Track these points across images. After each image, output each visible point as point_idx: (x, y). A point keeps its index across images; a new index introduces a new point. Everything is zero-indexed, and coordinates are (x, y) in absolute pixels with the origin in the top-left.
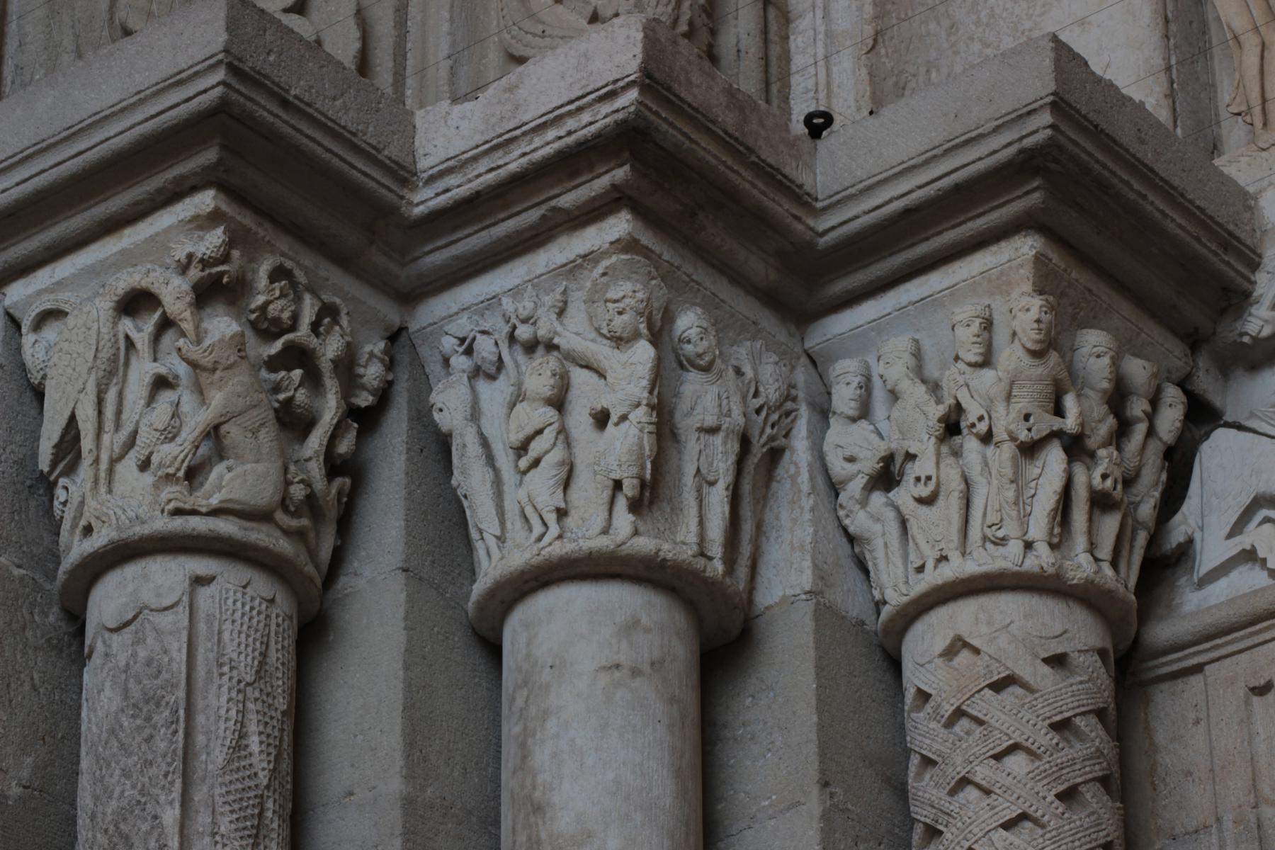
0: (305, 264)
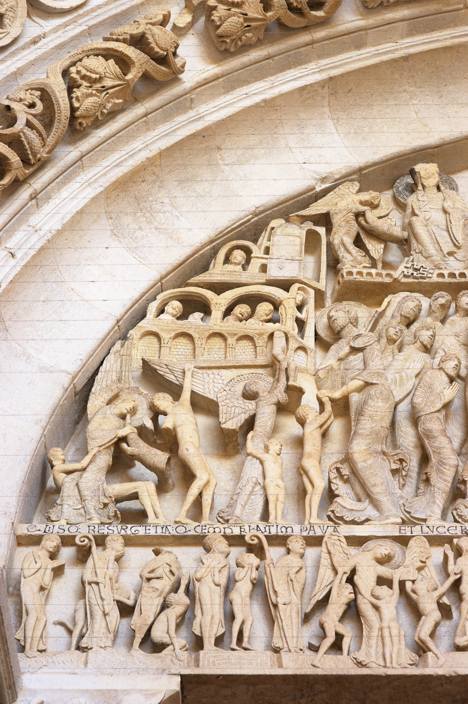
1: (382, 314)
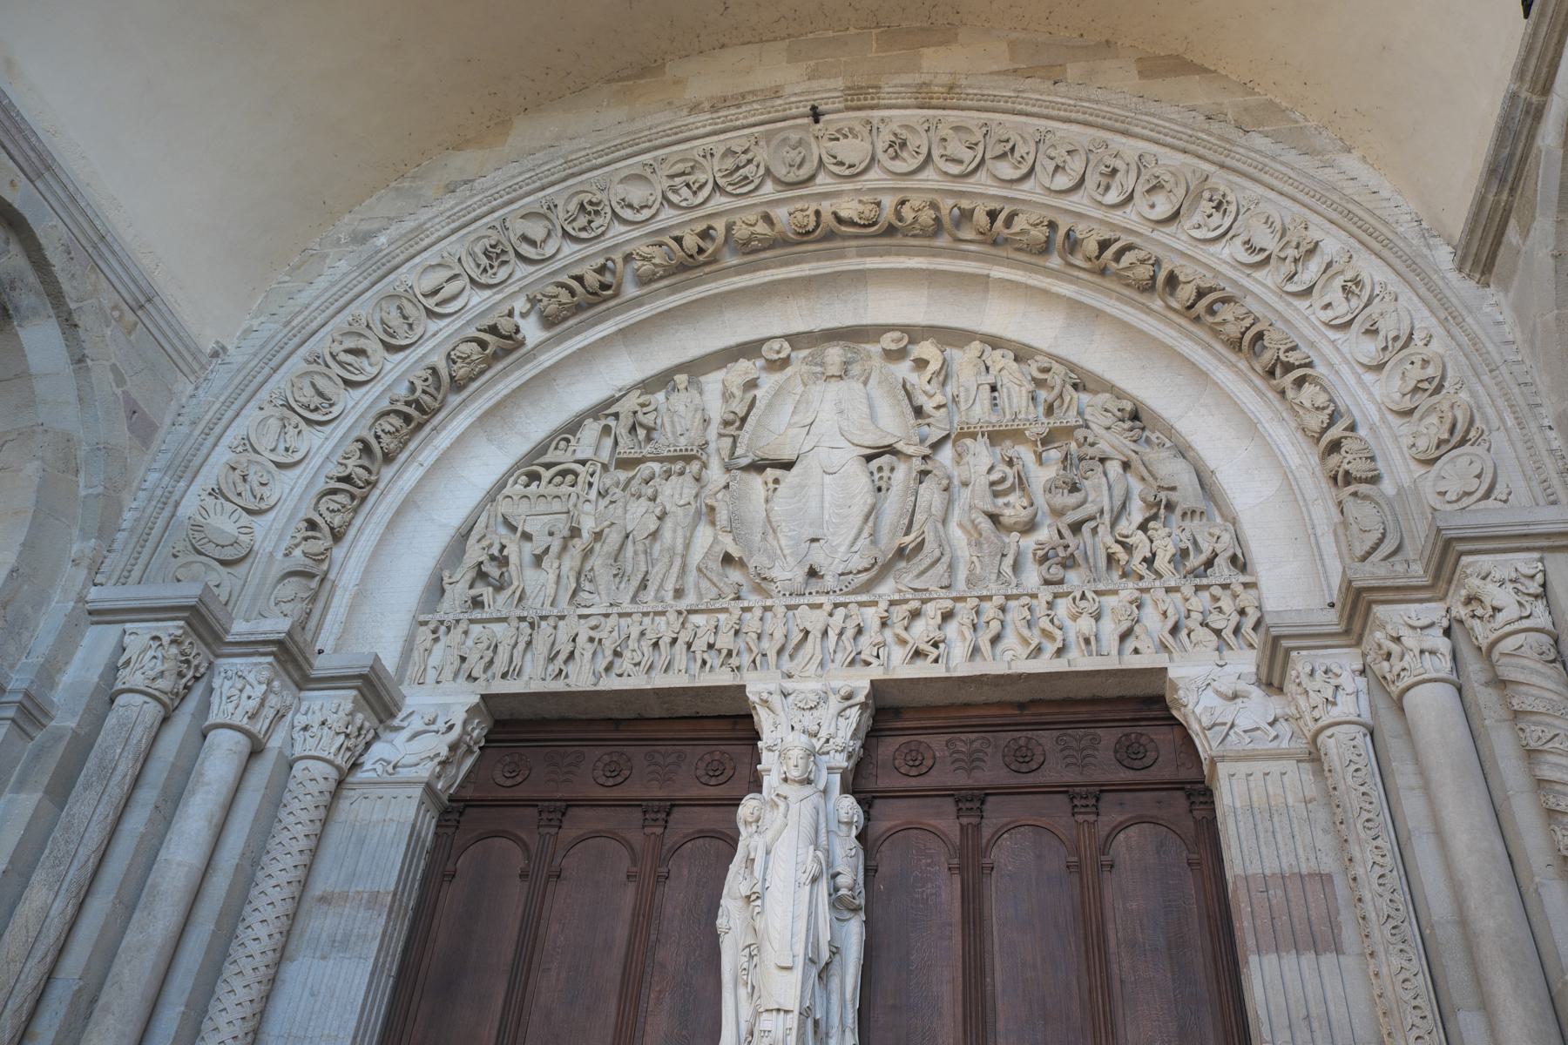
1: (633, 478)
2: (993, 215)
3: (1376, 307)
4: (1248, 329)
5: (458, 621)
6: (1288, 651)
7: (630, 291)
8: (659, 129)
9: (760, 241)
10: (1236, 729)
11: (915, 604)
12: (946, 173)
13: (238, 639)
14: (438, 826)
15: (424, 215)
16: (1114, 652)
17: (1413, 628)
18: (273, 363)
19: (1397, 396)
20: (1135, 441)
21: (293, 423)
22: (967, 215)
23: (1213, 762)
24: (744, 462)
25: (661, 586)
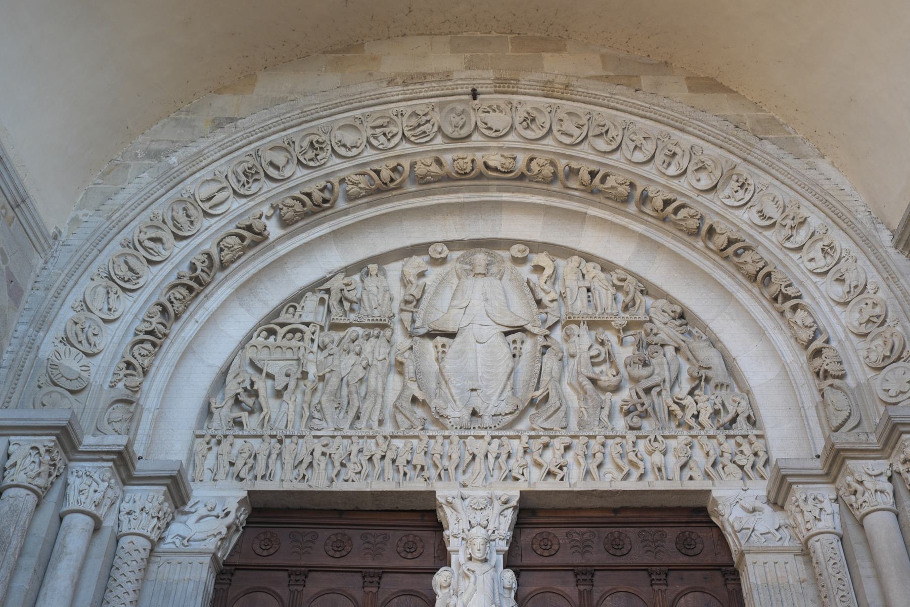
0: (61, 452)
2: (593, 174)
3: (843, 265)
4: (761, 269)
5: (226, 436)
6: (791, 484)
7: (341, 204)
8: (367, 94)
9: (432, 176)
10: (756, 532)
11: (545, 440)
12: (561, 142)
13: (89, 449)
14: (216, 583)
15: (203, 144)
16: (677, 477)
17: (870, 475)
18: (100, 247)
19: (856, 324)
20: (683, 334)
21: (114, 291)
22: (573, 172)
23: (742, 554)
24: (423, 331)
25: (370, 418)
